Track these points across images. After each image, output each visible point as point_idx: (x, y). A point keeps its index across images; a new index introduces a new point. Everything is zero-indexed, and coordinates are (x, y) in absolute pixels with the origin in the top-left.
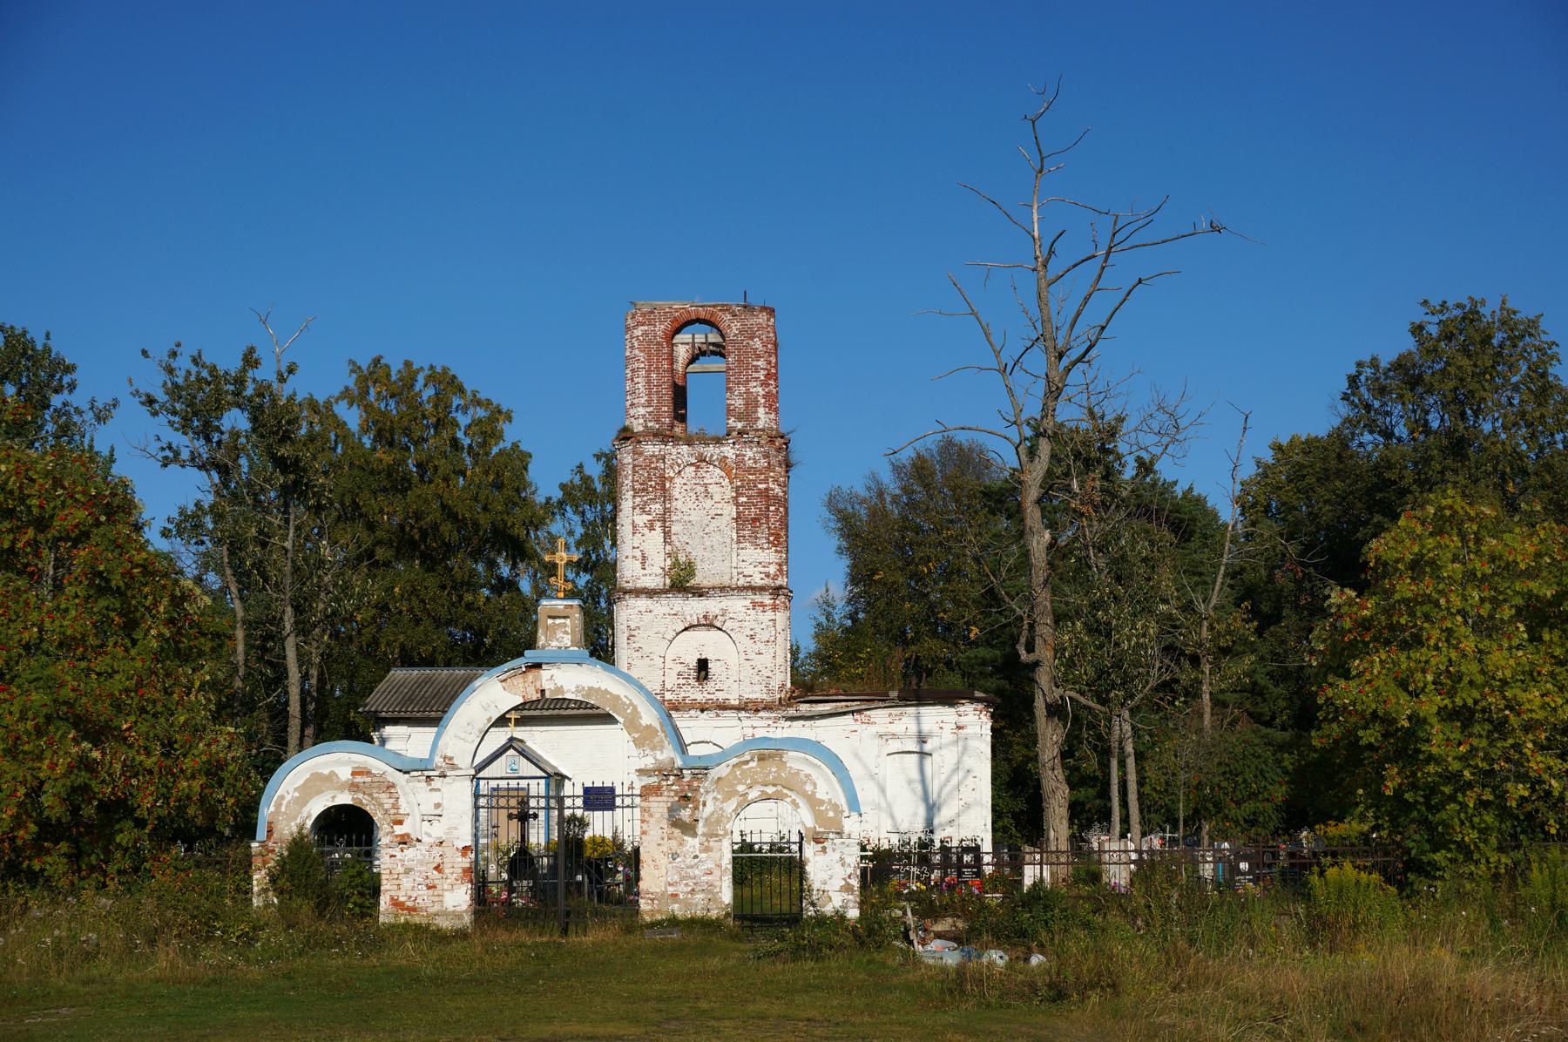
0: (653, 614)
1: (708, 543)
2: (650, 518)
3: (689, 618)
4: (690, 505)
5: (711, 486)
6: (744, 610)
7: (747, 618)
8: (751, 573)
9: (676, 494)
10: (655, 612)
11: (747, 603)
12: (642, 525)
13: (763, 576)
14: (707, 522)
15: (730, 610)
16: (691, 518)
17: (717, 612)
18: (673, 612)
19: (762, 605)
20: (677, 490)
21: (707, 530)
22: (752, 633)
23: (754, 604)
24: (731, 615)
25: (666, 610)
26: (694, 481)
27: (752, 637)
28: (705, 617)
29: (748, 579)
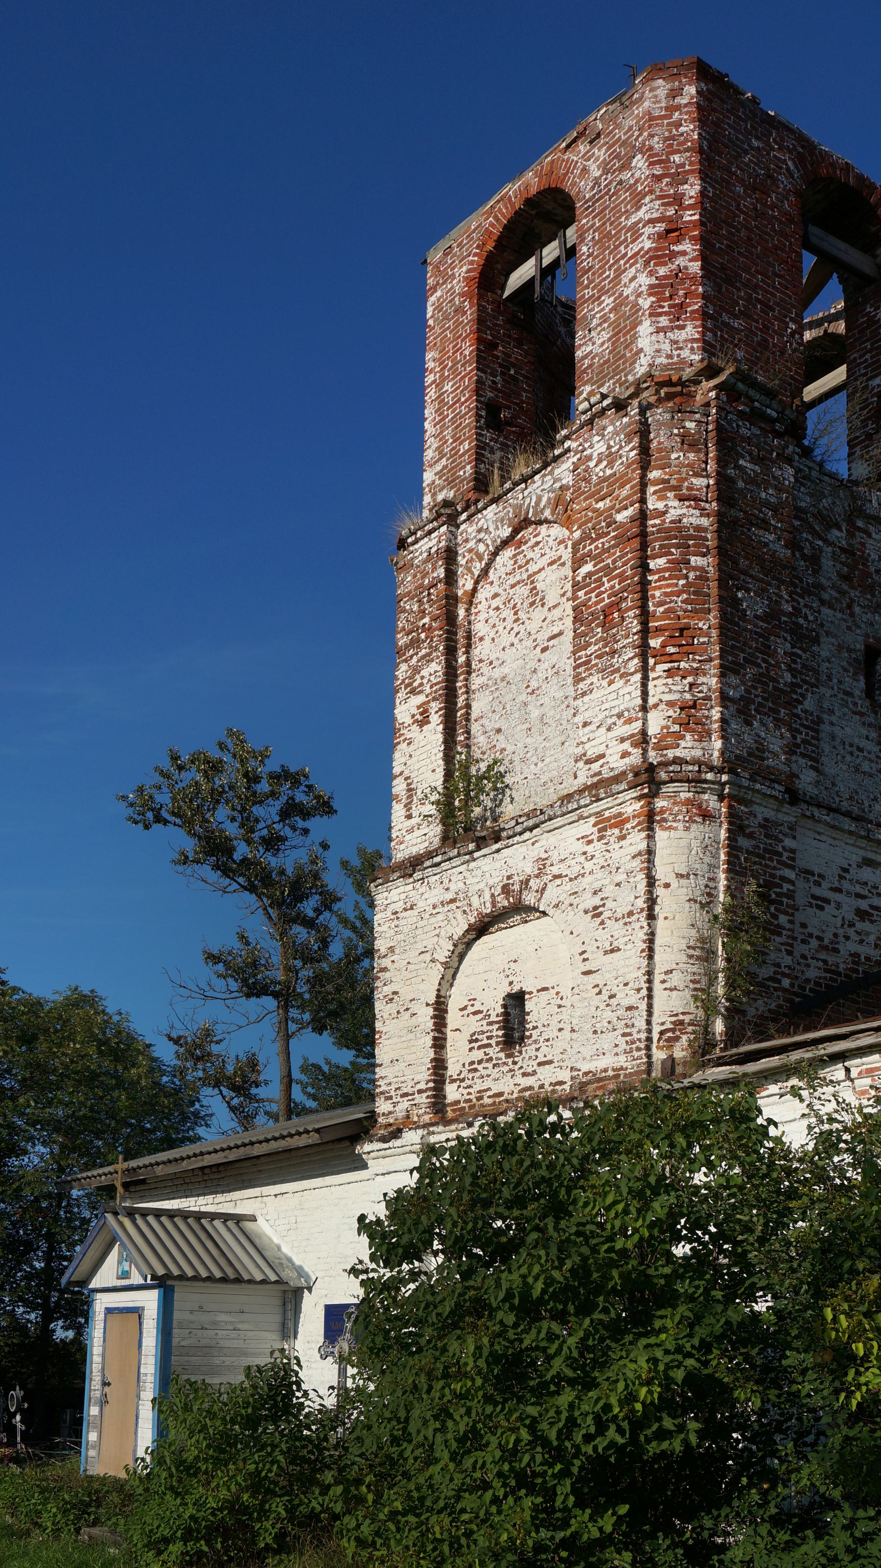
0: (415, 912)
1: (535, 713)
2: (421, 699)
3: (476, 902)
4: (506, 639)
5: (542, 576)
6: (581, 847)
7: (589, 866)
8: (601, 749)
9: (480, 628)
10: (421, 905)
11: (587, 828)
12: (408, 720)
13: (626, 746)
14: (532, 664)
15: (555, 858)
16: (505, 670)
17: (528, 871)
18: (449, 896)
19: (620, 822)
20: (482, 616)
21: (534, 684)
22: (597, 901)
23: (604, 824)
24: (555, 870)
25: (436, 895)
26: (512, 581)
27: (596, 912)
28: (506, 890)
29: (596, 767)
